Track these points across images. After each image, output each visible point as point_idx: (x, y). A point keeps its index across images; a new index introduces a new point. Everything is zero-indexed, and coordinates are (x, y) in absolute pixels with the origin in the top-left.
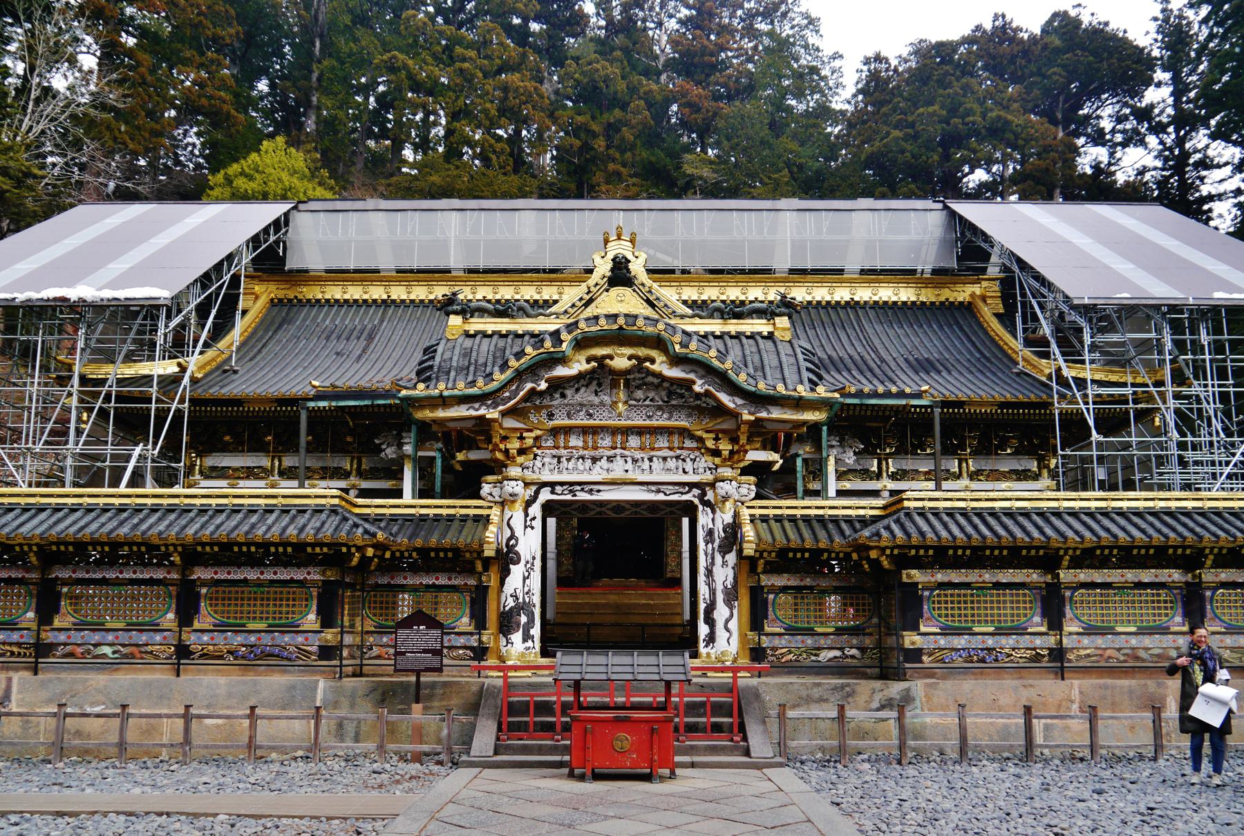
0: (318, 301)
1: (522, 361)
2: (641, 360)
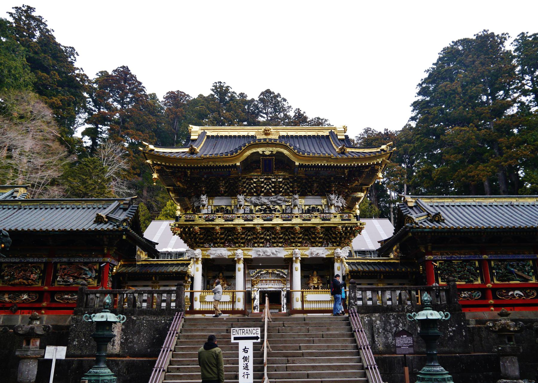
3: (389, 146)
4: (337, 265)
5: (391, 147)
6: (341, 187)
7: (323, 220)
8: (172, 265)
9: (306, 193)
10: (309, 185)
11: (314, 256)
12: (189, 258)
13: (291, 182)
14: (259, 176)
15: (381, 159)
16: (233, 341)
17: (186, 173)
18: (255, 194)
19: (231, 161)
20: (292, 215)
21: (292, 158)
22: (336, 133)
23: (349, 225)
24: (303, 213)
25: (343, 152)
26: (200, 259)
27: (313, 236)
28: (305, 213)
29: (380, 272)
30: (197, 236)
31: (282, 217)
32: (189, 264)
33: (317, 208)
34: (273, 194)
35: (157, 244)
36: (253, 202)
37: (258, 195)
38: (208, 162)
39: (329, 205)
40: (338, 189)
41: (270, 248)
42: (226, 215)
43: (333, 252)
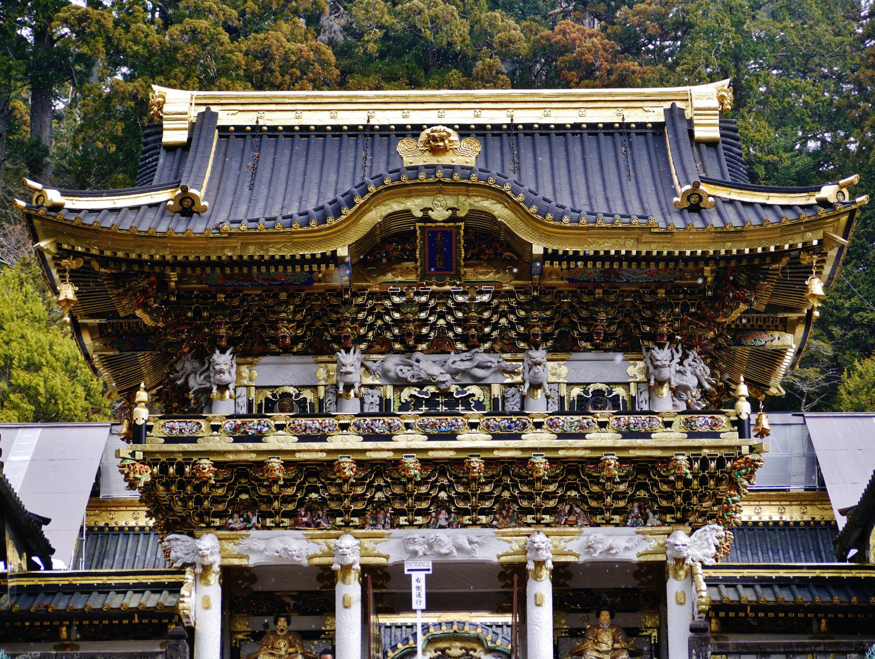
0: (132, 529)
1: (396, 653)
2: (467, 650)
3: (849, 186)
4: (674, 587)
5: (855, 192)
6: (690, 323)
7: (626, 435)
8: (122, 589)
9: (575, 340)
10: (584, 314)
11: (597, 556)
12: (178, 564)
13: (521, 305)
14: (410, 284)
15: (820, 234)
16: (406, 572)
17: (162, 284)
18: (397, 346)
19: (319, 243)
20: (524, 419)
21: (523, 233)
22: (688, 114)
23: (713, 452)
24: (561, 412)
25: (698, 204)
26: (216, 568)
27: (595, 488)
28: (571, 413)
29: (815, 608)
30: (205, 490)
31: (488, 427)
32: (181, 584)
33: (610, 392)
34: (459, 346)
35: (47, 521)
36: (392, 374)
37: (410, 350)
38: (245, 245)
39: (652, 382)
40: (682, 328)
41: (449, 531)
42: (303, 421)
43: (661, 542)
